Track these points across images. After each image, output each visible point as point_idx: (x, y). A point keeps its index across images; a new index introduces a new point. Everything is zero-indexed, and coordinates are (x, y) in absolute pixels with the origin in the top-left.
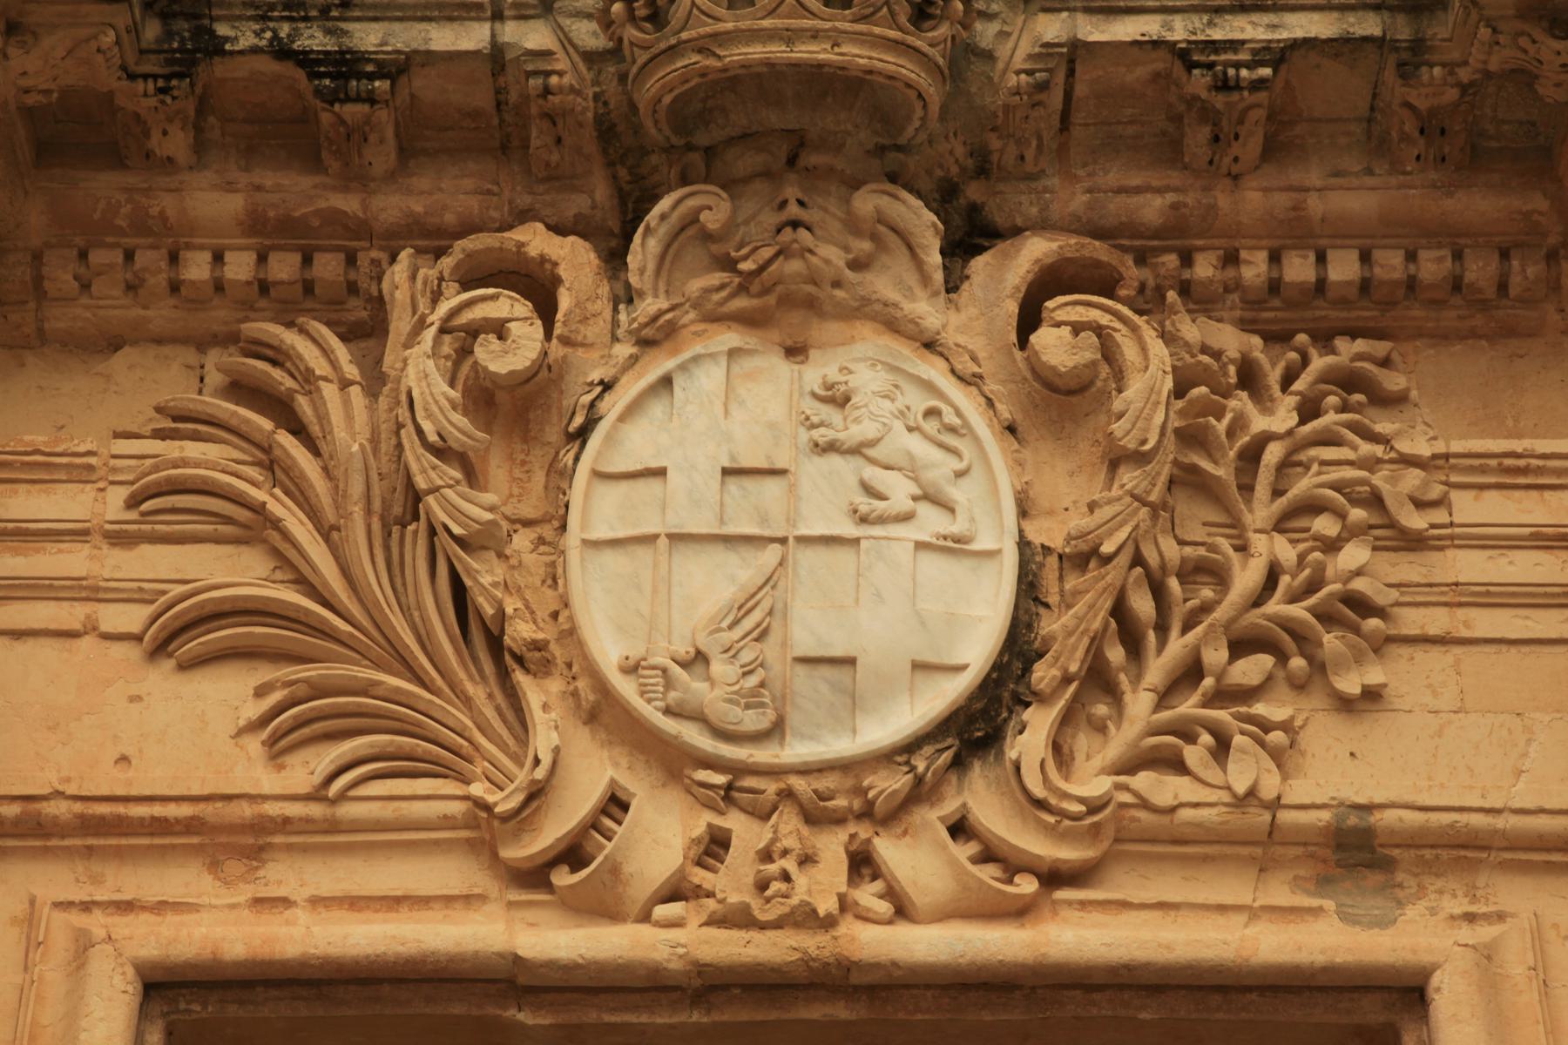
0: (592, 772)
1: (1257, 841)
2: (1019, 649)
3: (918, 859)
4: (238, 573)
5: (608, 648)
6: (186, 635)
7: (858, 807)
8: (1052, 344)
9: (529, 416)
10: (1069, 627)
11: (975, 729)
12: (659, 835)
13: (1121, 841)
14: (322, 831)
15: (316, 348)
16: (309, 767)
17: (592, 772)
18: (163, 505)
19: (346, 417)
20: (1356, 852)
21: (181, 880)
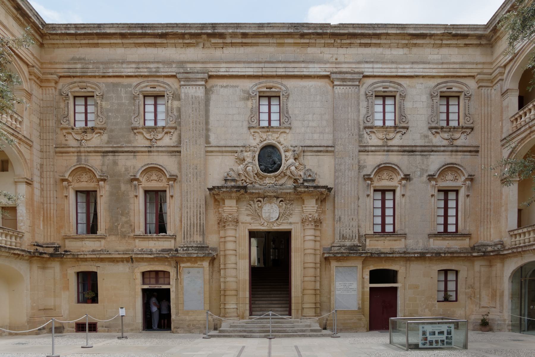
0: (263, 221)
1: (287, 223)
2: (279, 216)
3: (275, 224)
4: (249, 212)
5: (264, 217)
6: (248, 215)
7: (273, 223)
8: (281, 204)
9: (261, 207)
10: (281, 216)
11: (277, 219)
12: (266, 224)
13: (282, 223)
14: (254, 223)
15: (252, 203)
16: (253, 220)
17: (263, 221)
18: (246, 210)
19: (253, 206)
20: (291, 223)
21: (249, 225)
